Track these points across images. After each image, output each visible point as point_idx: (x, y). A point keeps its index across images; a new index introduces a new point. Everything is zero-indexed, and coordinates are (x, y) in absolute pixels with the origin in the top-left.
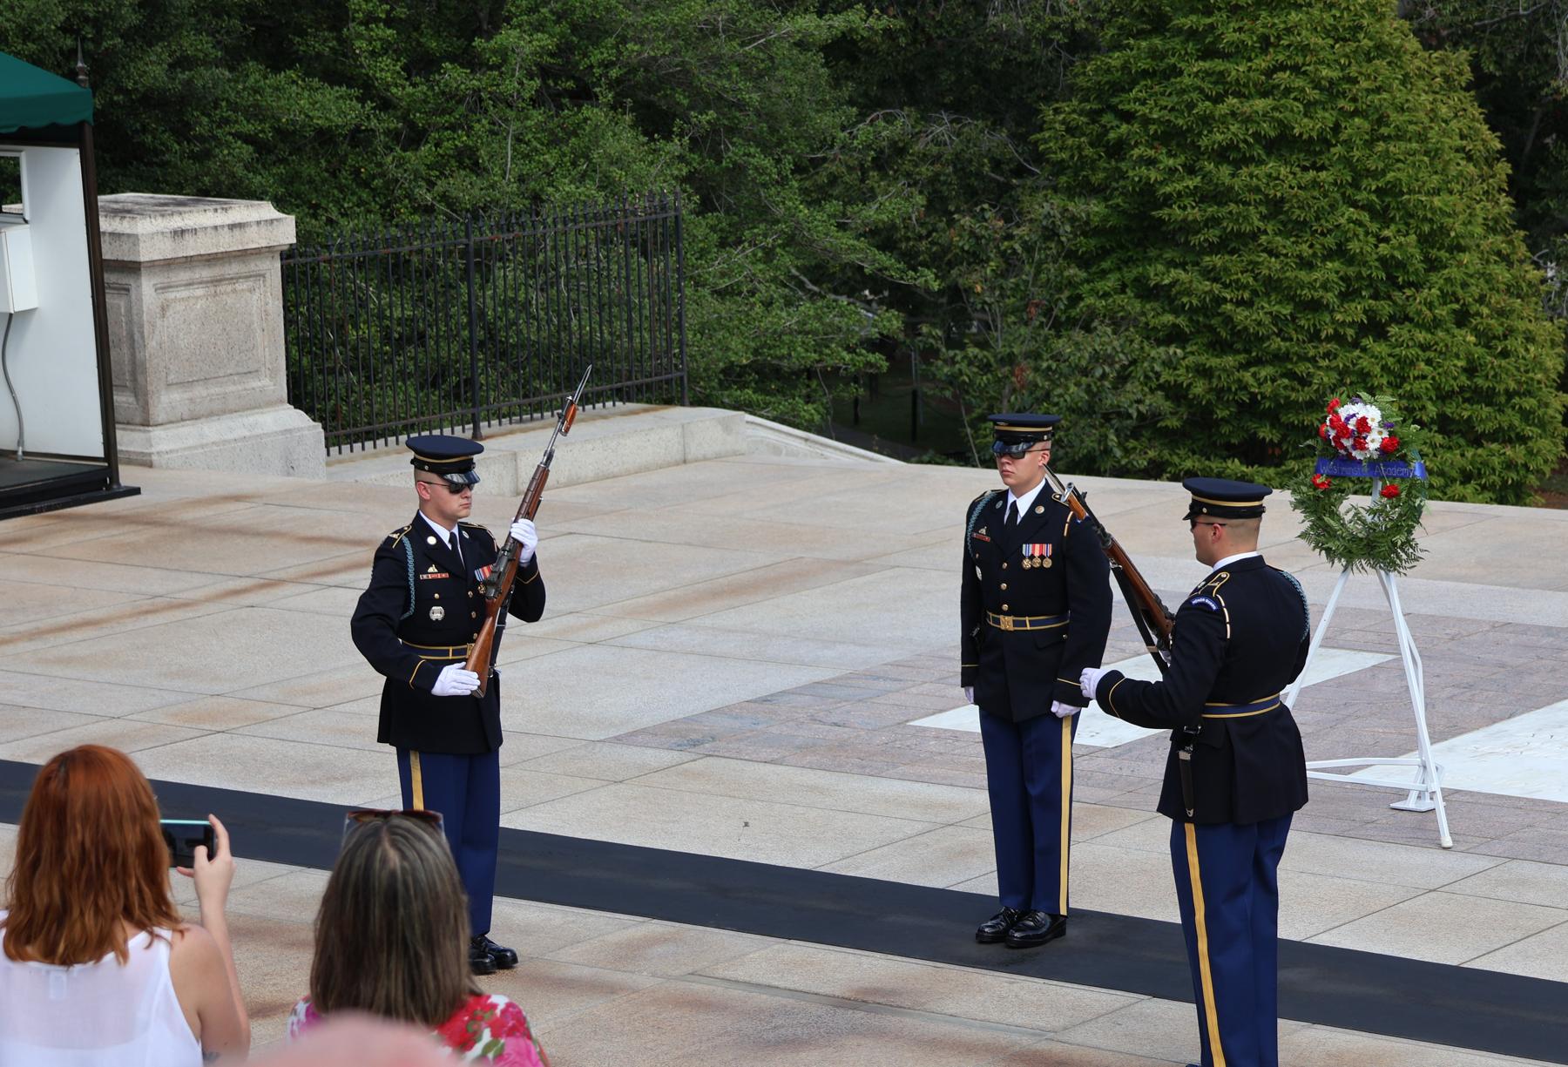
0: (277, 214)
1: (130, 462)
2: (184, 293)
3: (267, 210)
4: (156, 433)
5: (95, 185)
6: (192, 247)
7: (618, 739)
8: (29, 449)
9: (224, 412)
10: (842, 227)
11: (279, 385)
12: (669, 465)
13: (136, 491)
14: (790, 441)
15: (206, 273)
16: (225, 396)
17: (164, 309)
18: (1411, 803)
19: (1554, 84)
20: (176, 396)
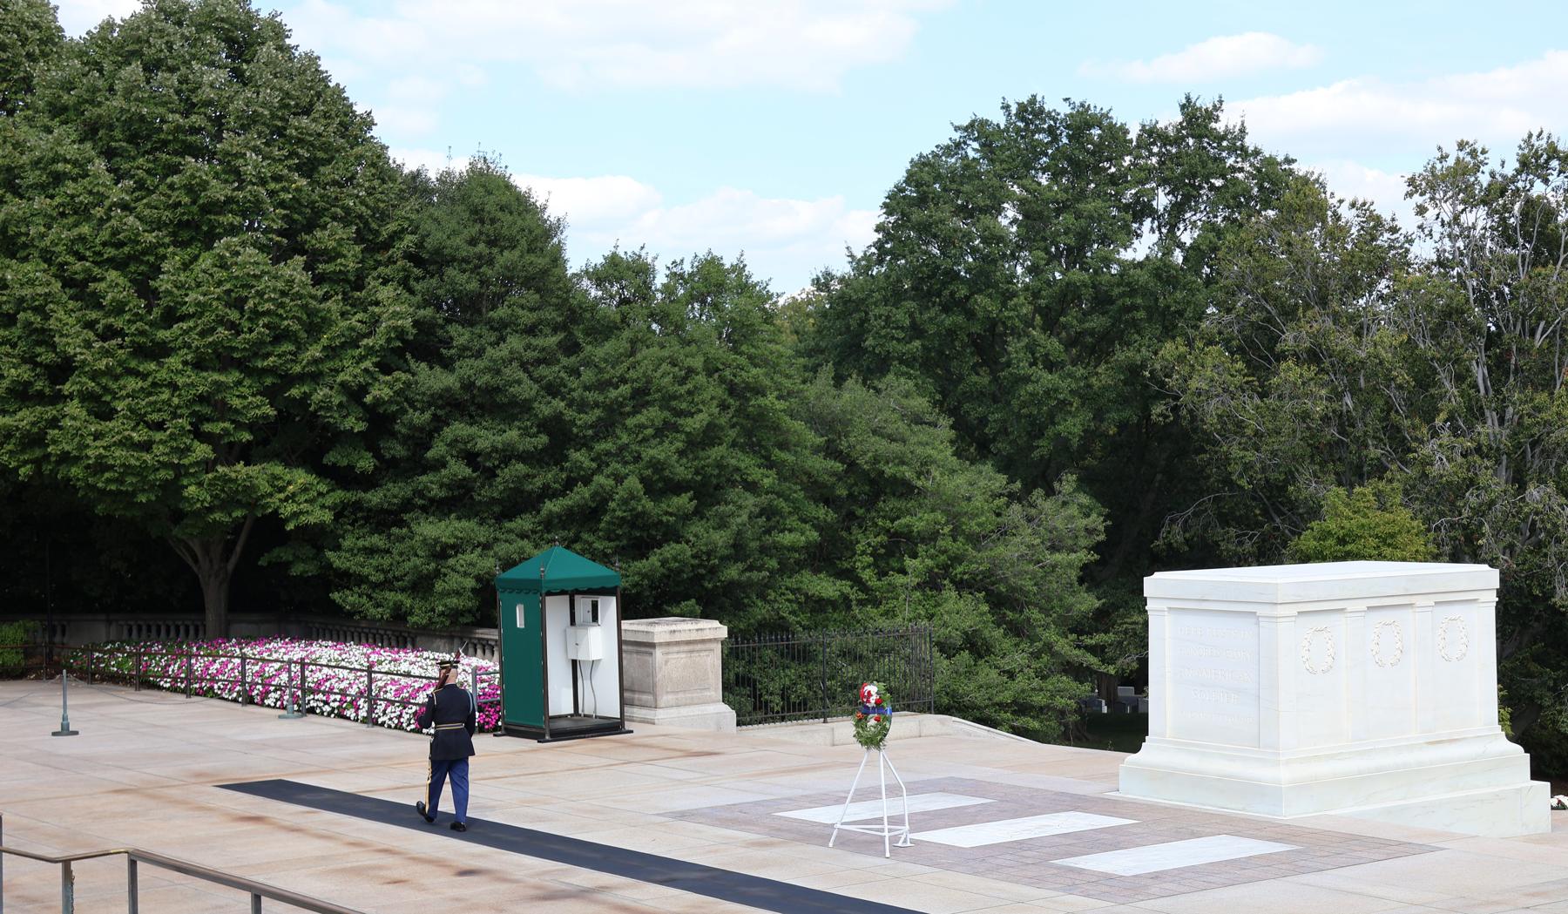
0: (720, 625)
1: (628, 720)
2: (675, 656)
3: (716, 623)
4: (659, 711)
5: (625, 613)
6: (678, 638)
7: (658, 815)
8: (586, 713)
9: (690, 704)
10: (1079, 647)
11: (718, 692)
12: (911, 737)
13: (632, 732)
14: (979, 731)
15: (686, 648)
16: (692, 698)
17: (666, 662)
18: (900, 844)
19: (1553, 600)
20: (670, 697)
